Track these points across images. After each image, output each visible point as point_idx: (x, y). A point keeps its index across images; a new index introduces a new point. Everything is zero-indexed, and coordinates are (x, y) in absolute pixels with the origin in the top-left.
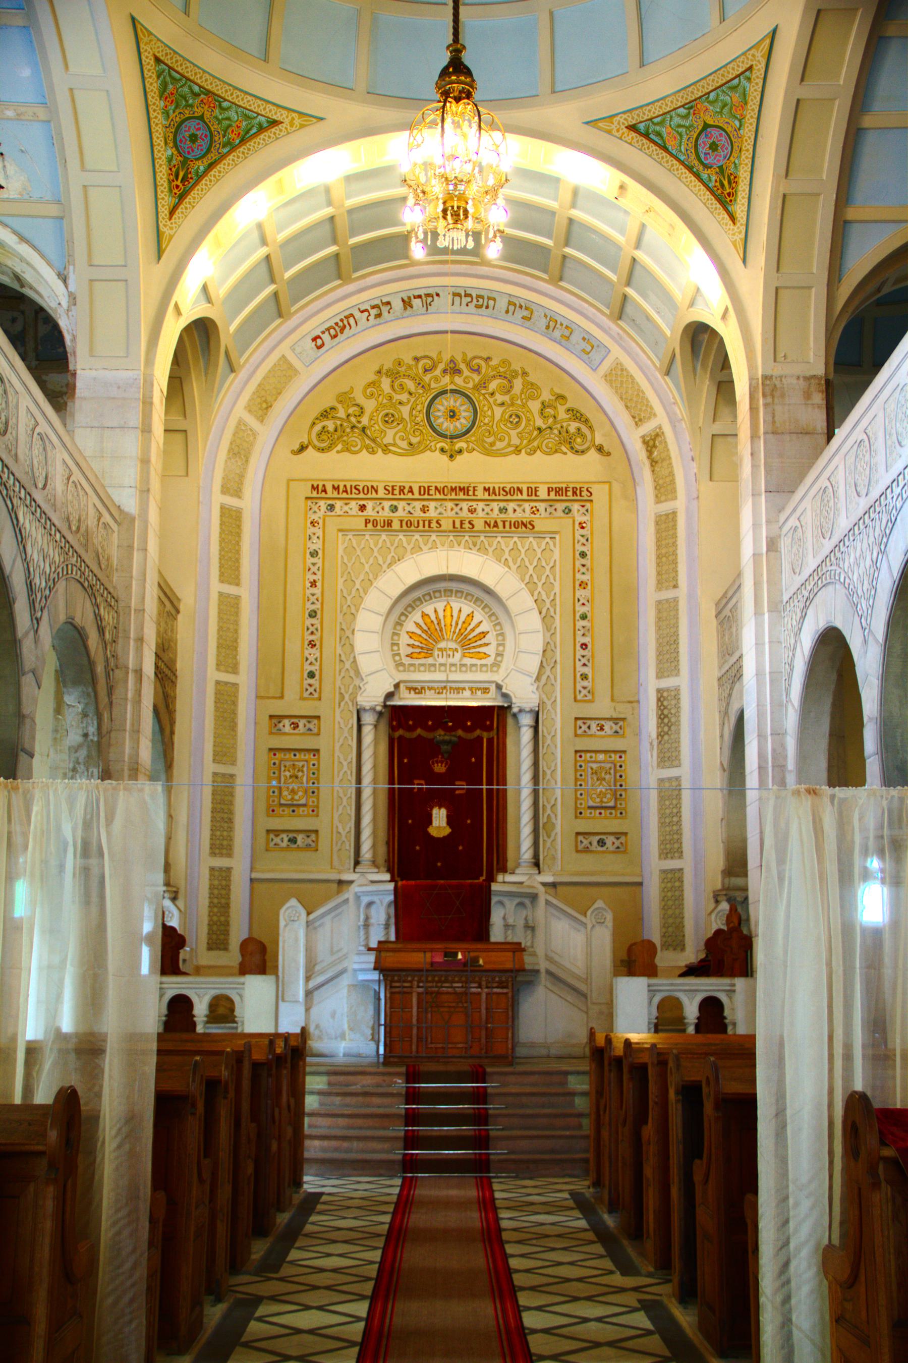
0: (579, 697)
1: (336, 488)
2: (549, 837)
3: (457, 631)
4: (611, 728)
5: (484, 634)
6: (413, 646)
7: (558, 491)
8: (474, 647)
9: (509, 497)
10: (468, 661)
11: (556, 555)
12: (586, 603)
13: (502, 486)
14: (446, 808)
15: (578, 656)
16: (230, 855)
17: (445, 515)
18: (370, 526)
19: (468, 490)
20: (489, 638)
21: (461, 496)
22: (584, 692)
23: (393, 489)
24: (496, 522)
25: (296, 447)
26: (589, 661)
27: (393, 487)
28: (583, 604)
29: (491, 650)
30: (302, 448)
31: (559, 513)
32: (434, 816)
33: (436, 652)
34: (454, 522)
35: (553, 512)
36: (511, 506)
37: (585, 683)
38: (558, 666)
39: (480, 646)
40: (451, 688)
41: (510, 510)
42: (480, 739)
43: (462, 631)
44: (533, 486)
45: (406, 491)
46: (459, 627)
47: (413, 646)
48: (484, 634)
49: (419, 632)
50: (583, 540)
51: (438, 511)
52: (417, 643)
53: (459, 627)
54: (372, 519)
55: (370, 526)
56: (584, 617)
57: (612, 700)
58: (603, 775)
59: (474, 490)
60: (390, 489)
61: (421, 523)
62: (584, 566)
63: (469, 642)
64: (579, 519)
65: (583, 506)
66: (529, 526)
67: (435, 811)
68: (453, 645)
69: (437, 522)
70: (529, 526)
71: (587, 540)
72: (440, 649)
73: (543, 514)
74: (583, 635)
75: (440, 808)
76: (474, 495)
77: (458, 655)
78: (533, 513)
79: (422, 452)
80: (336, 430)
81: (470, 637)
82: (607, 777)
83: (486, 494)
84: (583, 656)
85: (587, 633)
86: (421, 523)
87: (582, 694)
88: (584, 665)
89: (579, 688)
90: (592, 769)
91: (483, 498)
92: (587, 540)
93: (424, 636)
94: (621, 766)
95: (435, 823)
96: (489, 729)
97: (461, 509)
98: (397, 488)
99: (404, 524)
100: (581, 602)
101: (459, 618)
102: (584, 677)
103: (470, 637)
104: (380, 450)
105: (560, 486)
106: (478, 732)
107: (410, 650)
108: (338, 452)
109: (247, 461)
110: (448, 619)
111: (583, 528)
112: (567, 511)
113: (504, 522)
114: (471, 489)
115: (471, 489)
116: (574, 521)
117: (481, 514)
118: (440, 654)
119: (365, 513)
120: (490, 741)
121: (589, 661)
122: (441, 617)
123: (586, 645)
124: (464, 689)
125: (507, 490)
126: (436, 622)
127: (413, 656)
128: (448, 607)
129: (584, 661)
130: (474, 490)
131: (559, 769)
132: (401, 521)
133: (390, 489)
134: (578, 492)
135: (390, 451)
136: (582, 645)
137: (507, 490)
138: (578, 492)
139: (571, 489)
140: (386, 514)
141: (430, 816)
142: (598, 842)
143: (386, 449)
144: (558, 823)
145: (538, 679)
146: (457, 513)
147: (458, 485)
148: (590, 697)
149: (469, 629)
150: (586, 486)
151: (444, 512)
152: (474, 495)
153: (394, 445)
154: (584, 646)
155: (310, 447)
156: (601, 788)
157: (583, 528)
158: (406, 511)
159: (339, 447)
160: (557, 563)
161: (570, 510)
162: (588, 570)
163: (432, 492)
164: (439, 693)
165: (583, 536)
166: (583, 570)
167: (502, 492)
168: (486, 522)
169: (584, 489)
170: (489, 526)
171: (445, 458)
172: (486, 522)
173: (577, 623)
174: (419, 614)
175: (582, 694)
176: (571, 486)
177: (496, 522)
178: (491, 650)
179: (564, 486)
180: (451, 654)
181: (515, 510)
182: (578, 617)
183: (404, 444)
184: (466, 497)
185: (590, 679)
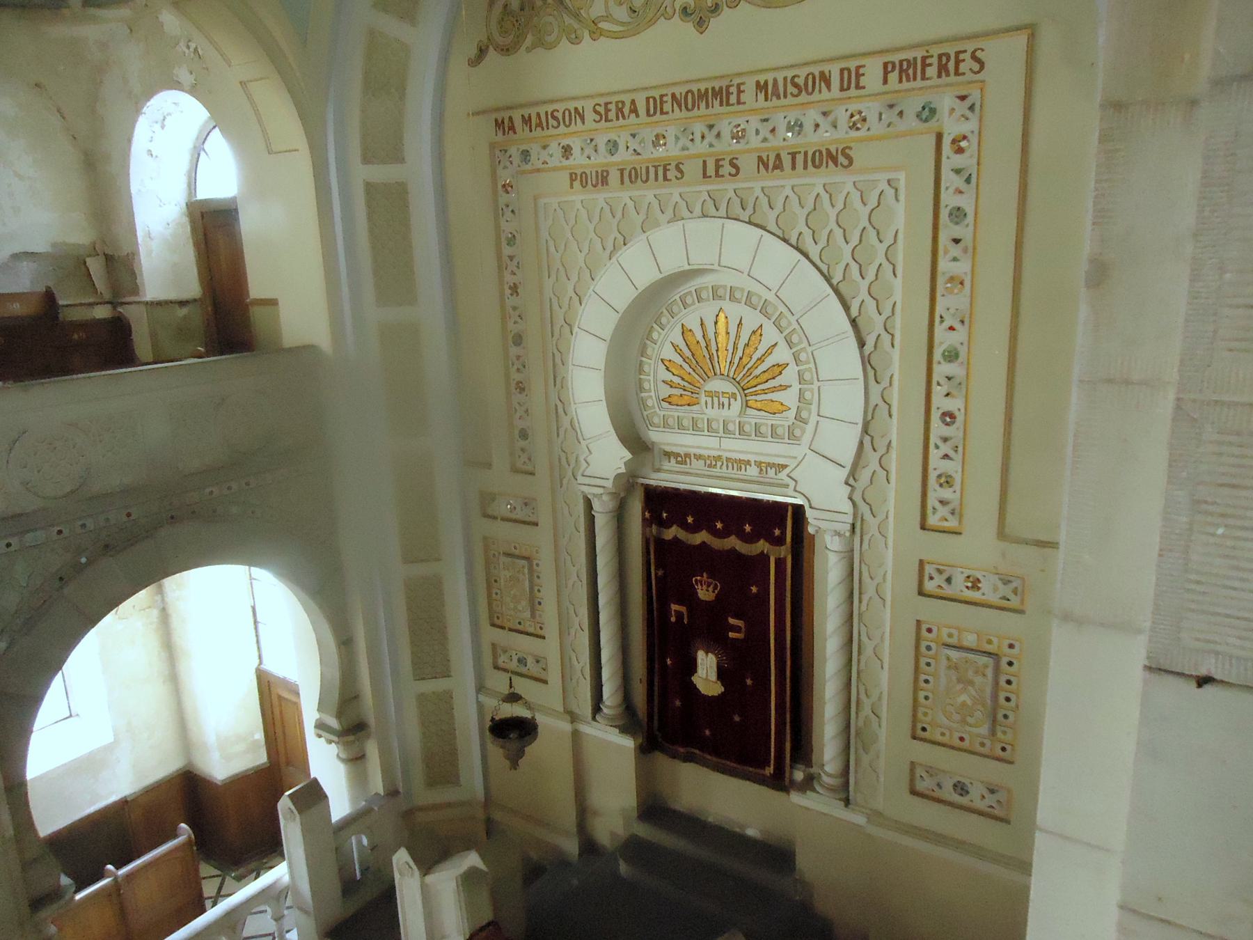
0: (932, 520)
1: (527, 121)
2: (866, 750)
3: (736, 361)
4: (995, 589)
5: (780, 367)
6: (671, 385)
7: (908, 70)
8: (764, 392)
9: (804, 98)
10: (753, 417)
11: (900, 222)
12: (957, 326)
13: (790, 74)
14: (716, 655)
15: (933, 439)
16: (446, 674)
17: (693, 151)
18: (577, 184)
19: (728, 94)
20: (789, 376)
21: (717, 108)
22: (943, 511)
23: (607, 111)
24: (778, 156)
25: (473, 52)
26: (956, 449)
27: (606, 104)
28: (952, 328)
29: (789, 398)
30: (482, 52)
31: (911, 122)
32: (699, 661)
33: (703, 399)
34: (705, 162)
35: (895, 119)
36: (812, 115)
37: (946, 494)
38: (893, 454)
39: (774, 389)
40: (728, 459)
41: (808, 127)
42: (764, 558)
43: (745, 360)
44: (852, 65)
45: (626, 110)
46: (739, 353)
47: (671, 385)
48: (780, 367)
49: (679, 360)
50: (958, 182)
51: (680, 144)
52: (677, 380)
53: (739, 353)
54: (579, 172)
55: (577, 184)
56: (951, 356)
57: (1002, 534)
58: (970, 674)
59: (740, 92)
60: (601, 110)
61: (652, 170)
62: (957, 241)
63: (753, 382)
64: (951, 129)
65: (963, 98)
66: (841, 159)
67: (701, 655)
68: (729, 387)
69: (677, 168)
70: (841, 159)
71: (968, 181)
72: (710, 394)
73: (877, 128)
74: (948, 395)
75: (707, 653)
76: (739, 103)
77: (737, 405)
78: (854, 127)
79: (652, 22)
80: (522, 9)
81: (757, 372)
82: (978, 680)
83: (761, 96)
84: (945, 440)
85: (954, 392)
86: (652, 170)
87: (938, 515)
88: (946, 456)
89: (932, 501)
90: (948, 659)
91: (756, 105)
92: (968, 181)
93: (686, 366)
94: (1010, 664)
95: (701, 671)
96: (780, 541)
97: (718, 135)
98: (612, 107)
99: (626, 174)
100: (947, 324)
101: (738, 336)
102: (947, 481)
103: (757, 372)
104: (586, 34)
105: (909, 55)
106: (762, 546)
107: (665, 391)
108: (528, 50)
109: (402, 96)
110: (722, 338)
111: (960, 151)
112: (926, 114)
113: (793, 156)
114: (733, 90)
115: (733, 90)
116: (939, 137)
117: (755, 142)
118: (709, 400)
119: (571, 162)
120: (780, 563)
121: (956, 449)
122: (711, 335)
123: (952, 416)
124: (748, 462)
125: (801, 81)
126: (703, 344)
127: (673, 400)
128: (722, 315)
129: (945, 448)
130: (740, 92)
131: (887, 643)
132: (622, 171)
133: (601, 110)
134: (951, 65)
135: (602, 33)
136: (944, 414)
137: (801, 81)
138: (951, 65)
139: (934, 61)
140: (602, 159)
141: (695, 660)
142: (955, 785)
143: (596, 33)
144: (883, 734)
145: (853, 474)
146: (711, 145)
147: (709, 85)
148: (952, 523)
149: (755, 358)
150: (970, 46)
151: (689, 144)
152: (739, 103)
153: (608, 17)
154: (948, 418)
155: (491, 48)
156: (963, 698)
157: (960, 151)
158: (631, 150)
159: (529, 39)
160: (900, 236)
161: (933, 111)
162: (965, 250)
163: (667, 107)
164: (710, 466)
165: (958, 171)
166: (955, 251)
167: (791, 89)
168: (760, 158)
169: (967, 56)
170: (766, 166)
171: (689, 28)
172: (760, 158)
173: (935, 366)
174: (678, 330)
175: (938, 515)
176: (936, 51)
177: (778, 156)
178: (789, 398)
179: (919, 54)
180: (726, 401)
181: (817, 126)
182: (937, 355)
183: (621, 13)
184: (725, 109)
185: (957, 487)
